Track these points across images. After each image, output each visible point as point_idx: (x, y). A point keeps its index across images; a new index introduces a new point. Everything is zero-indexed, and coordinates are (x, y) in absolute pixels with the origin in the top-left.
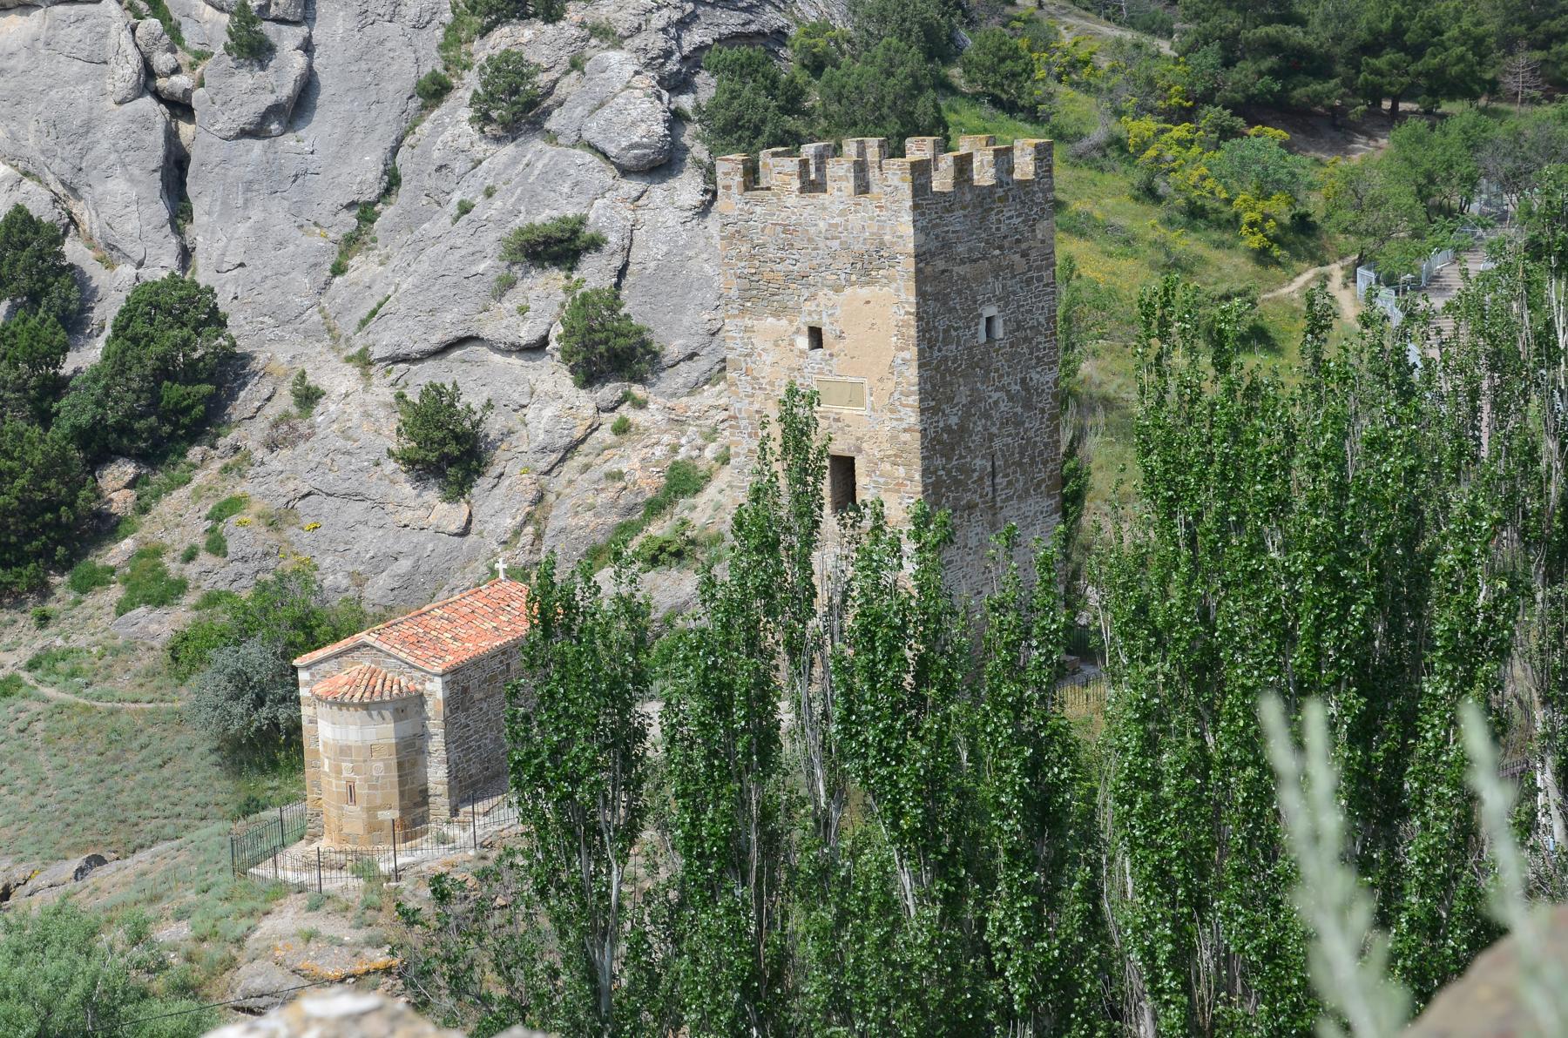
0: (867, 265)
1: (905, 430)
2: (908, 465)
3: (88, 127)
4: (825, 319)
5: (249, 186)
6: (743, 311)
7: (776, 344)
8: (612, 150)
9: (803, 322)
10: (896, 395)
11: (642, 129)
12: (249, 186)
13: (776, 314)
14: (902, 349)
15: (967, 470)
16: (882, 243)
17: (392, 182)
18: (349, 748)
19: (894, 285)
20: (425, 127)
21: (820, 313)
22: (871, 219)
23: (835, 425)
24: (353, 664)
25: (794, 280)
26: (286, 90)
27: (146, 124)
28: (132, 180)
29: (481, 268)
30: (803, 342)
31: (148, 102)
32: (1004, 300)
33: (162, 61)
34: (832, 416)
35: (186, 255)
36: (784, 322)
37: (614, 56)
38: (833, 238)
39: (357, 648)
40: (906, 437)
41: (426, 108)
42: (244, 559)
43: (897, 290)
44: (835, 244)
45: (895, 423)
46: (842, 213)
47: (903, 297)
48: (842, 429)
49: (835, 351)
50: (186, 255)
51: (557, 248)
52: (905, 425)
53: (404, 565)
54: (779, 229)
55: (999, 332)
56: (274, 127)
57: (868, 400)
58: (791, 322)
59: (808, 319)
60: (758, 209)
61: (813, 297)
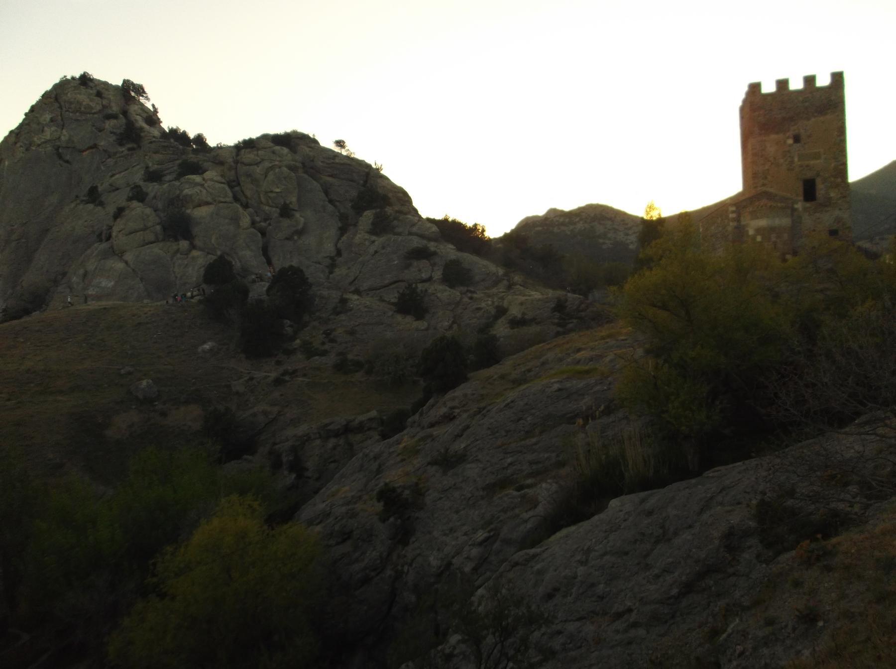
13: (777, 133)
17: (339, 253)
30: (790, 141)
31: (252, 230)
41: (342, 235)
44: (807, 104)
56: (296, 237)
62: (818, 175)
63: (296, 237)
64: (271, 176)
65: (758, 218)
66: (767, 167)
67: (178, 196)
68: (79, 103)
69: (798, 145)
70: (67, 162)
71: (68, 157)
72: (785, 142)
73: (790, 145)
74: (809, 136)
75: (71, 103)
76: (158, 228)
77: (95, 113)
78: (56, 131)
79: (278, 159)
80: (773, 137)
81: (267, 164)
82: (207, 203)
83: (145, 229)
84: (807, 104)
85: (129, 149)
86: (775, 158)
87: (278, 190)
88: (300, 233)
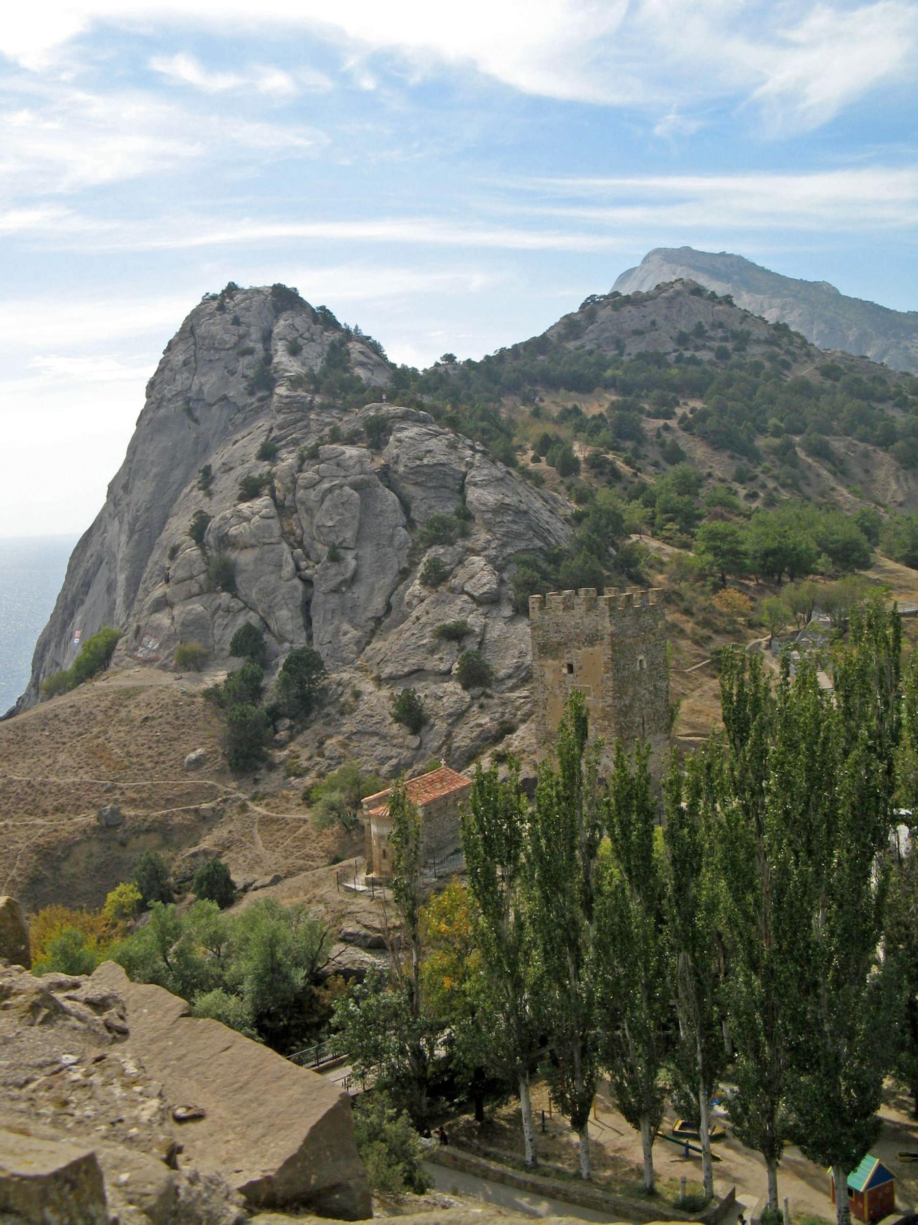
0: (592, 639)
2: (609, 720)
3: (274, 590)
5: (333, 611)
8: (476, 594)
9: (565, 662)
11: (488, 586)
12: (333, 611)
15: (633, 723)
17: (389, 608)
20: (402, 587)
26: (348, 575)
27: (295, 588)
28: (290, 610)
29: (424, 642)
30: (565, 671)
32: (647, 652)
33: (303, 564)
35: (310, 638)
37: (476, 558)
42: (332, 759)
46: (581, 618)
50: (310, 638)
51: (455, 634)
53: (394, 761)
55: (645, 666)
56: (344, 589)
63: (344, 589)
64: (327, 504)
67: (227, 534)
68: (213, 337)
69: (571, 675)
70: (196, 421)
71: (197, 414)
74: (581, 668)
75: (204, 338)
76: (202, 577)
77: (228, 349)
78: (188, 378)
79: (342, 474)
80: (550, 662)
81: (326, 485)
82: (253, 546)
83: (192, 577)
85: (261, 400)
87: (330, 524)
88: (353, 580)
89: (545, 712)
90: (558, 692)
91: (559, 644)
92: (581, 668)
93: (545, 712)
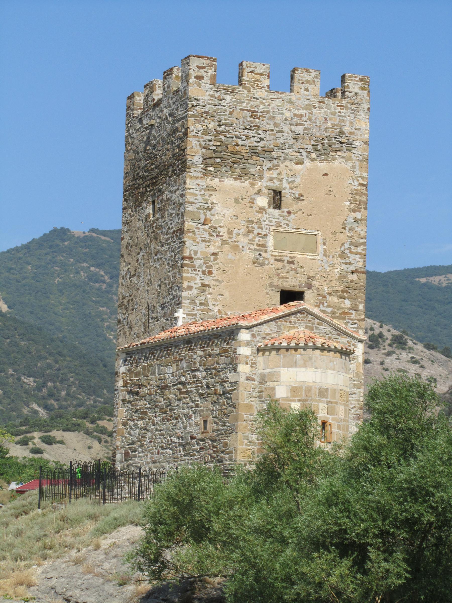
0: (328, 146)
1: (353, 272)
2: (354, 299)
4: (285, 184)
6: (206, 173)
7: (237, 201)
10: (347, 245)
13: (238, 178)
14: (354, 211)
16: (342, 132)
18: (326, 390)
19: (350, 164)
21: (281, 180)
22: (333, 114)
23: (288, 267)
24: (290, 328)
25: (258, 154)
30: (262, 201)
34: (286, 259)
36: (246, 184)
38: (297, 125)
39: (300, 312)
40: (354, 277)
43: (353, 167)
44: (300, 130)
45: (344, 266)
46: (307, 107)
47: (357, 173)
48: (295, 270)
49: (291, 209)
52: (353, 268)
54: (248, 114)
57: (321, 248)
58: (253, 185)
59: (269, 184)
60: (228, 98)
61: (275, 167)
62: (309, 286)
65: (295, 364)
66: (212, 249)
72: (252, 201)
73: (261, 210)
74: (299, 198)
80: (229, 182)
84: (300, 130)
86: (230, 232)
89: (208, 280)
90: (243, 241)
91: (253, 151)
92: (299, 198)
93: (208, 280)
